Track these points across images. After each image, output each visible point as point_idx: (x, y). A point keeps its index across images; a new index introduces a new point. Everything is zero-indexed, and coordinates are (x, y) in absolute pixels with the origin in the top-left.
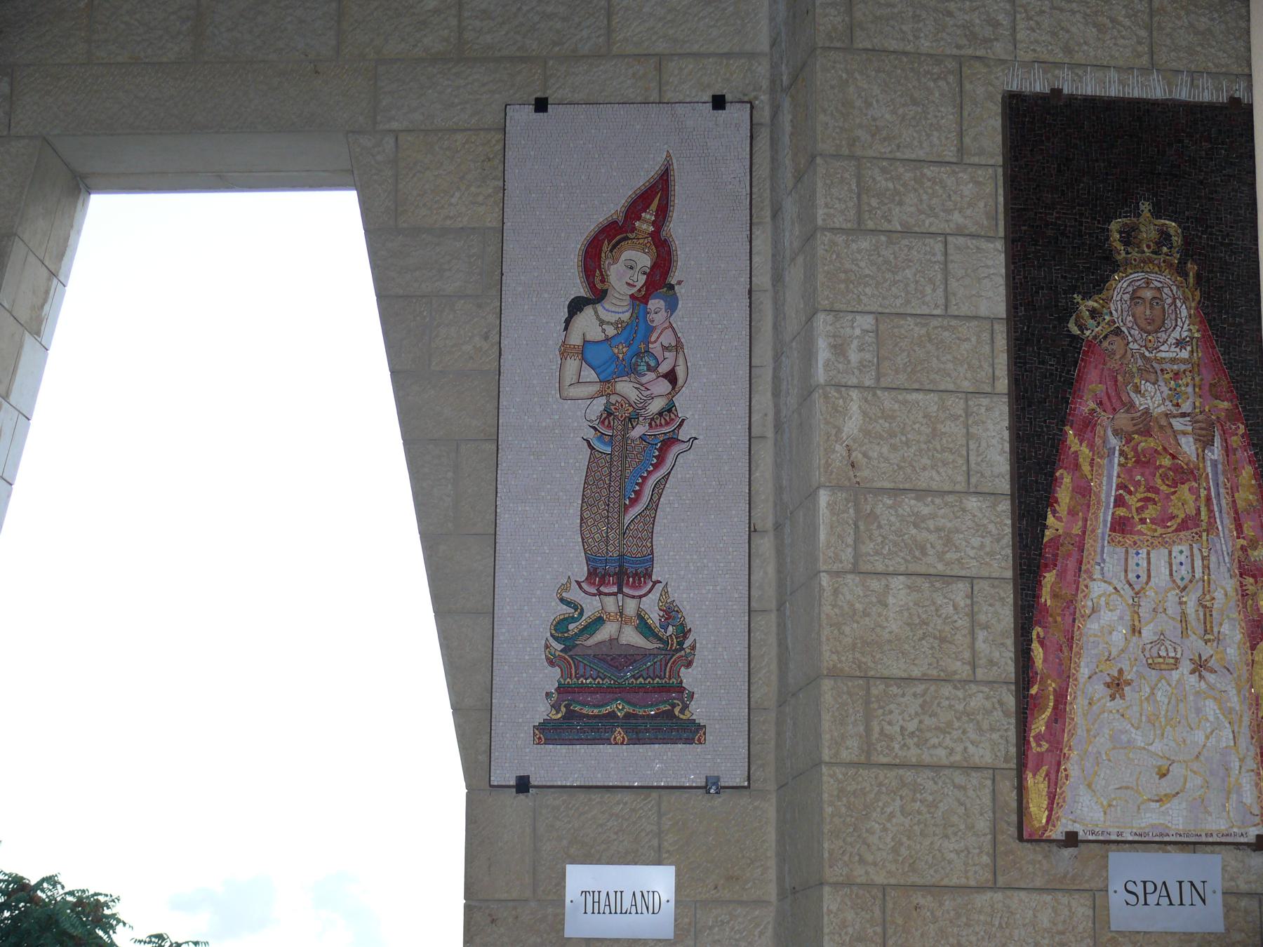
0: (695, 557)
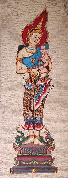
0: (55, 119)
